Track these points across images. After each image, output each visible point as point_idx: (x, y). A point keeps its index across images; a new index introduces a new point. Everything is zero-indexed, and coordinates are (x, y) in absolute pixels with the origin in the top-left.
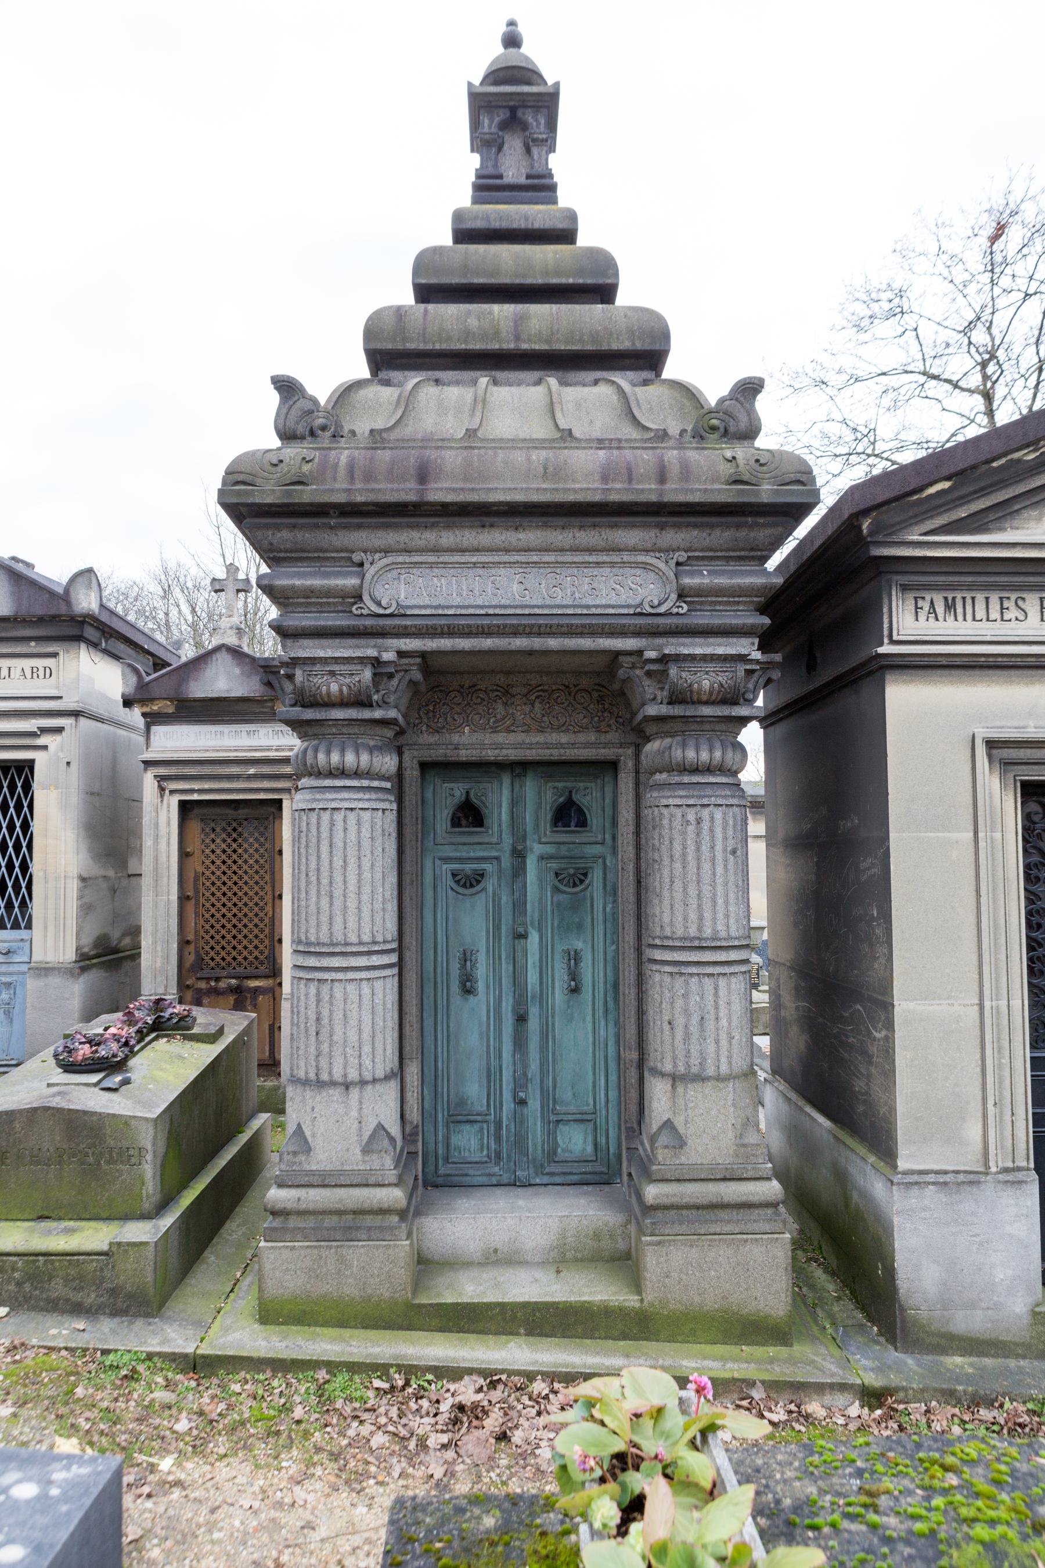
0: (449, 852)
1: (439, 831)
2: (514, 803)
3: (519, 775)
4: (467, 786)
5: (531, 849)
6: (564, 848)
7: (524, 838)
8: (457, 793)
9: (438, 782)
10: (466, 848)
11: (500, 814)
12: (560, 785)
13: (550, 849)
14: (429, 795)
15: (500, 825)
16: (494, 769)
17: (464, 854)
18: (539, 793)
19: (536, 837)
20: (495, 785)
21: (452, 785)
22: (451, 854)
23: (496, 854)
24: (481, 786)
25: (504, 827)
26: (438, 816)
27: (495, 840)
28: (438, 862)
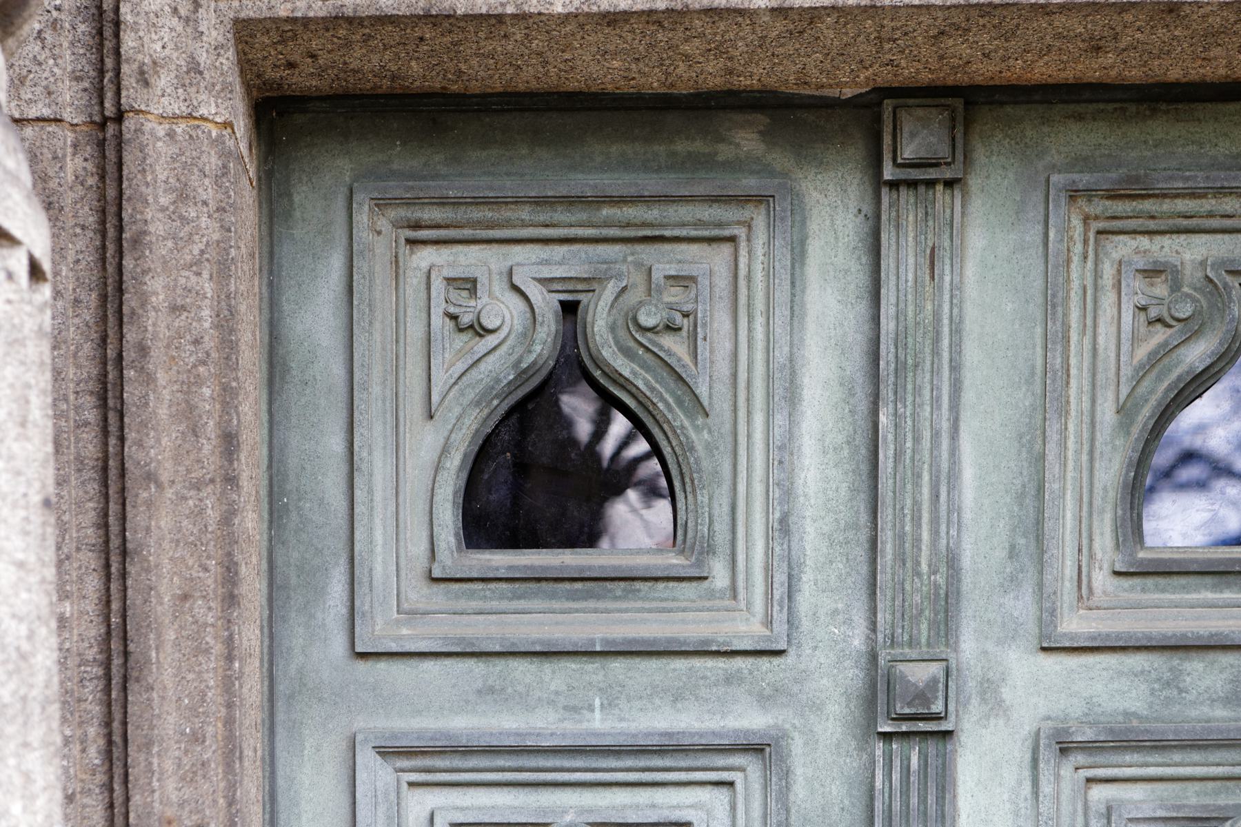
0: (446, 704)
1: (378, 562)
2: (880, 374)
3: (925, 180)
4: (568, 263)
5: (990, 689)
6: (1207, 676)
7: (946, 608)
8: (501, 310)
9: (377, 232)
10: (556, 676)
11: (783, 453)
12: (1192, 252)
13: (1111, 690)
14: (316, 320)
15: (784, 527)
16: (746, 140)
17: (545, 724)
18: (1052, 303)
19: (1022, 606)
20: (759, 247)
21: (467, 259)
22: (464, 724)
23: (750, 720)
24: (665, 260)
25: (812, 535)
26: (376, 465)
27: (746, 628)
28: (376, 775)
